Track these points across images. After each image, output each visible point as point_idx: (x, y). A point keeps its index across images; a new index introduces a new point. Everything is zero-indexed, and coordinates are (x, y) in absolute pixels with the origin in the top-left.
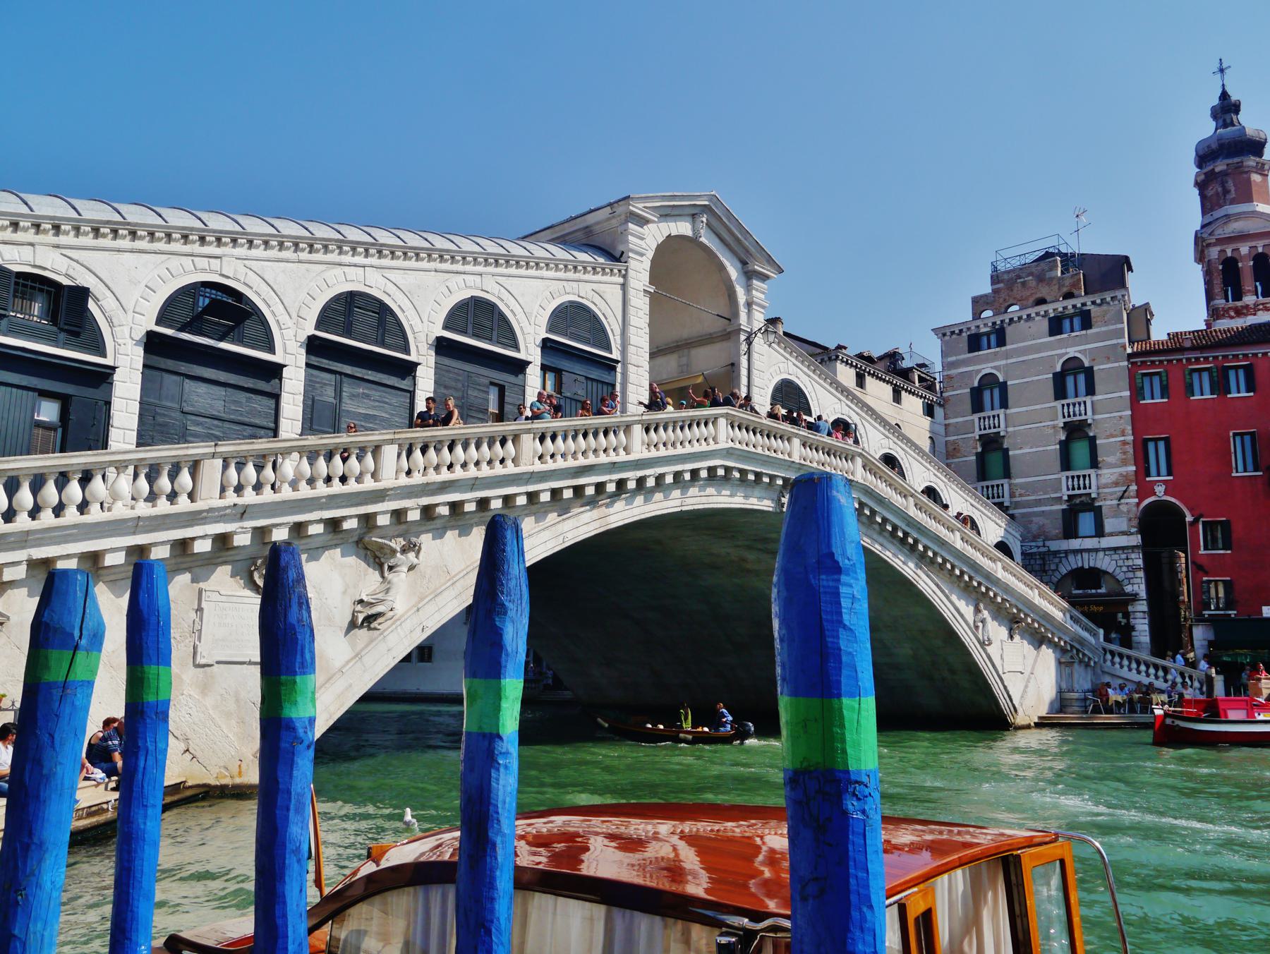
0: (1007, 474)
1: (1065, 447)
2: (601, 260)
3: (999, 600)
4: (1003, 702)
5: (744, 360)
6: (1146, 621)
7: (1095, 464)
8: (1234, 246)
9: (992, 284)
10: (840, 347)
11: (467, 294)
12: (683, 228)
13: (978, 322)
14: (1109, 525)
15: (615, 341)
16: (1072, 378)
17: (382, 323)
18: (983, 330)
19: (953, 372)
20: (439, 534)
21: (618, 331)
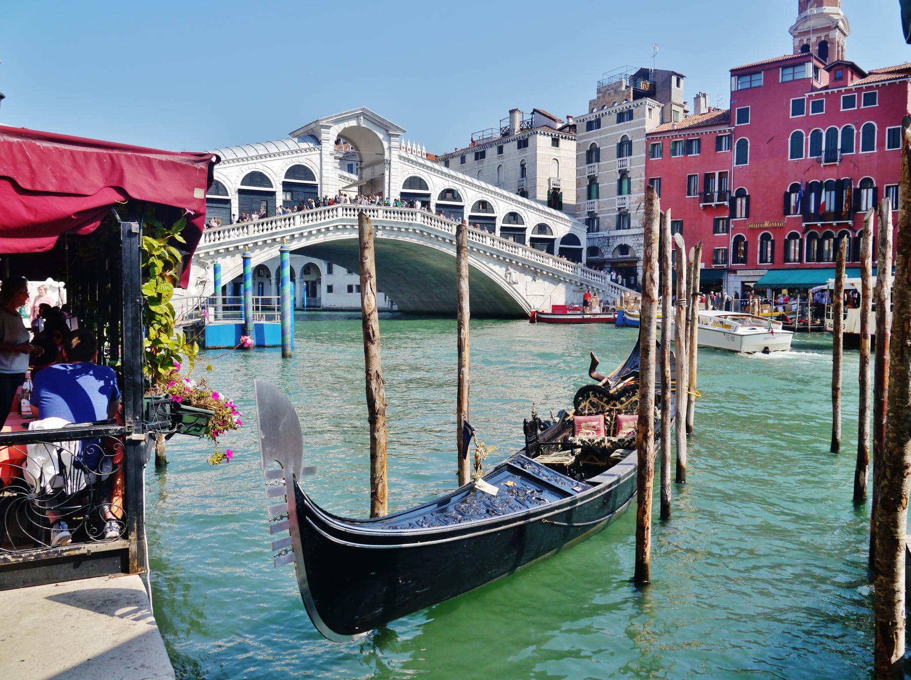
0: (598, 197)
1: (620, 182)
2: (312, 145)
4: (524, 307)
5: (387, 173)
7: (629, 192)
8: (807, 37)
10: (568, 117)
11: (250, 171)
12: (353, 123)
13: (590, 115)
14: (633, 223)
15: (317, 176)
16: (624, 147)
17: (217, 187)
18: (593, 119)
19: (580, 142)
20: (224, 257)
21: (318, 172)
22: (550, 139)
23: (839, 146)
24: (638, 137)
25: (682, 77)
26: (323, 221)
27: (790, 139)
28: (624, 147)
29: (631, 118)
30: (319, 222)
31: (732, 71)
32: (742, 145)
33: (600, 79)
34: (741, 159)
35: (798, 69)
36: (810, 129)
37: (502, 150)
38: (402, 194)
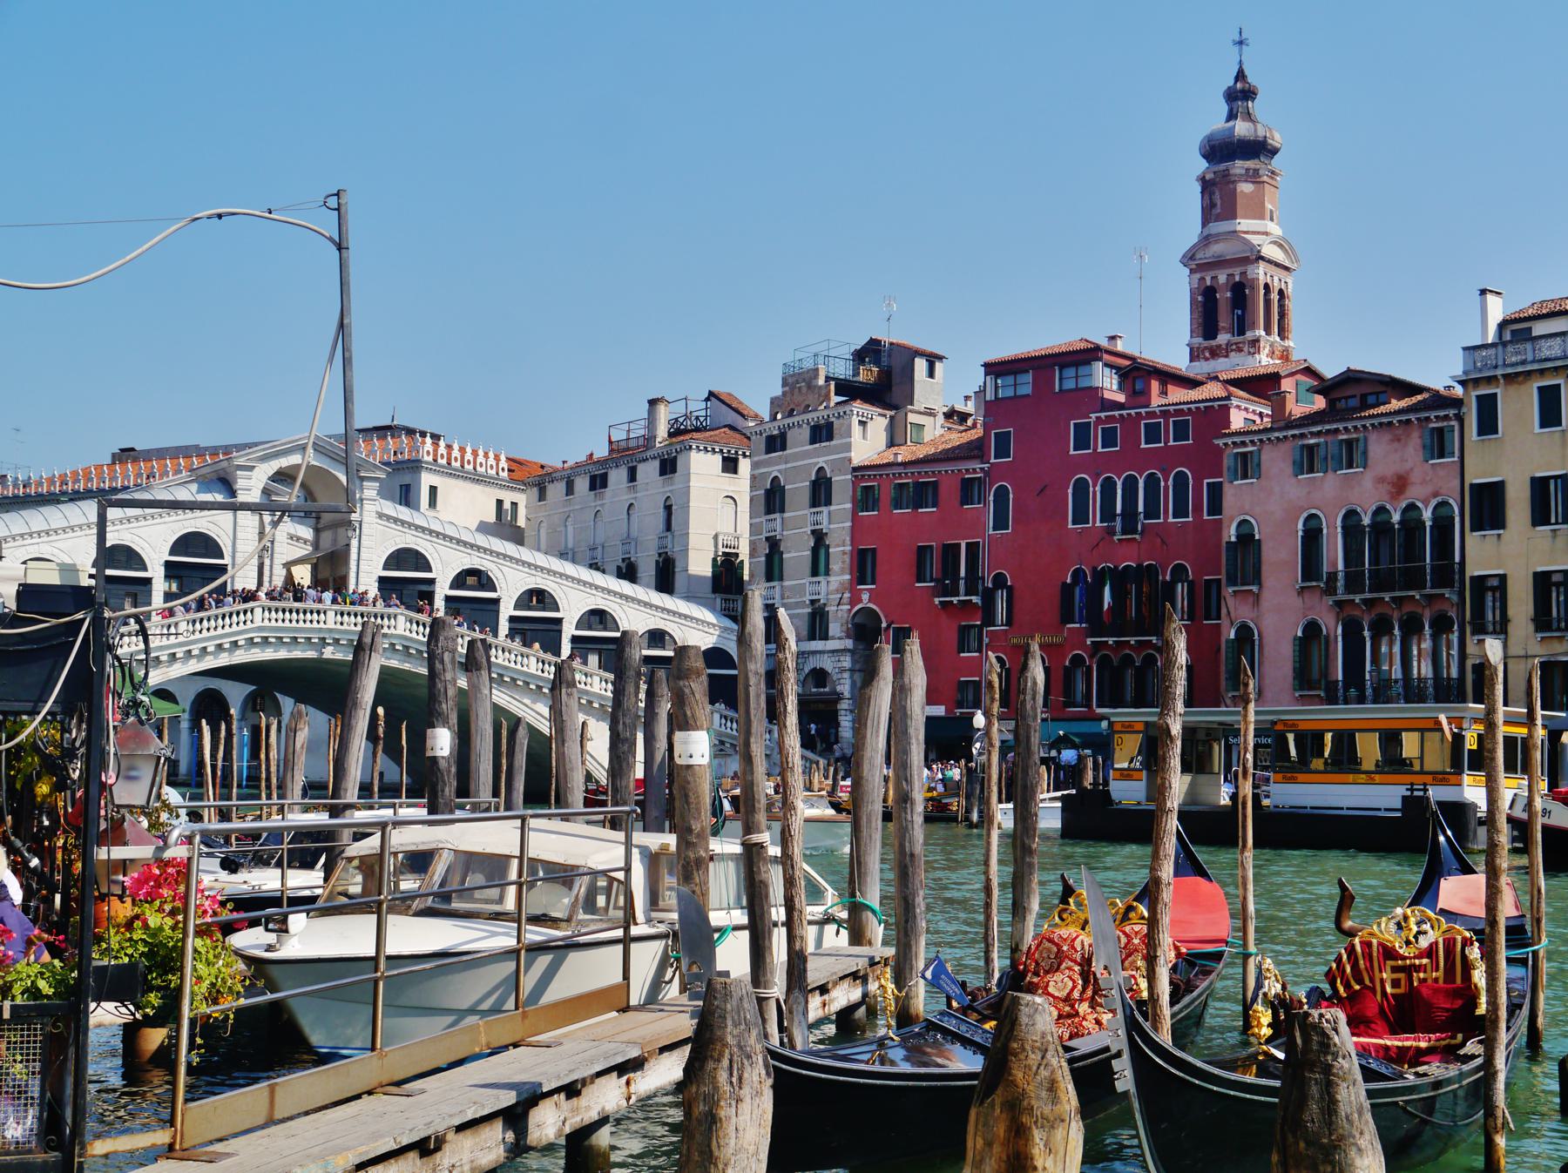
0: (781, 579)
3: (596, 705)
5: (354, 543)
6: (849, 718)
7: (827, 573)
8: (1212, 273)
9: (784, 385)
14: (835, 628)
15: (227, 551)
21: (229, 544)
22: (719, 458)
23: (1141, 508)
24: (841, 473)
25: (940, 358)
26: (227, 630)
27: (1070, 491)
28: (821, 491)
29: (830, 438)
30: (220, 631)
31: (986, 365)
32: (1001, 494)
33: (789, 359)
34: (1000, 523)
35: (1082, 370)
36: (1098, 475)
37: (611, 490)
38: (382, 580)
